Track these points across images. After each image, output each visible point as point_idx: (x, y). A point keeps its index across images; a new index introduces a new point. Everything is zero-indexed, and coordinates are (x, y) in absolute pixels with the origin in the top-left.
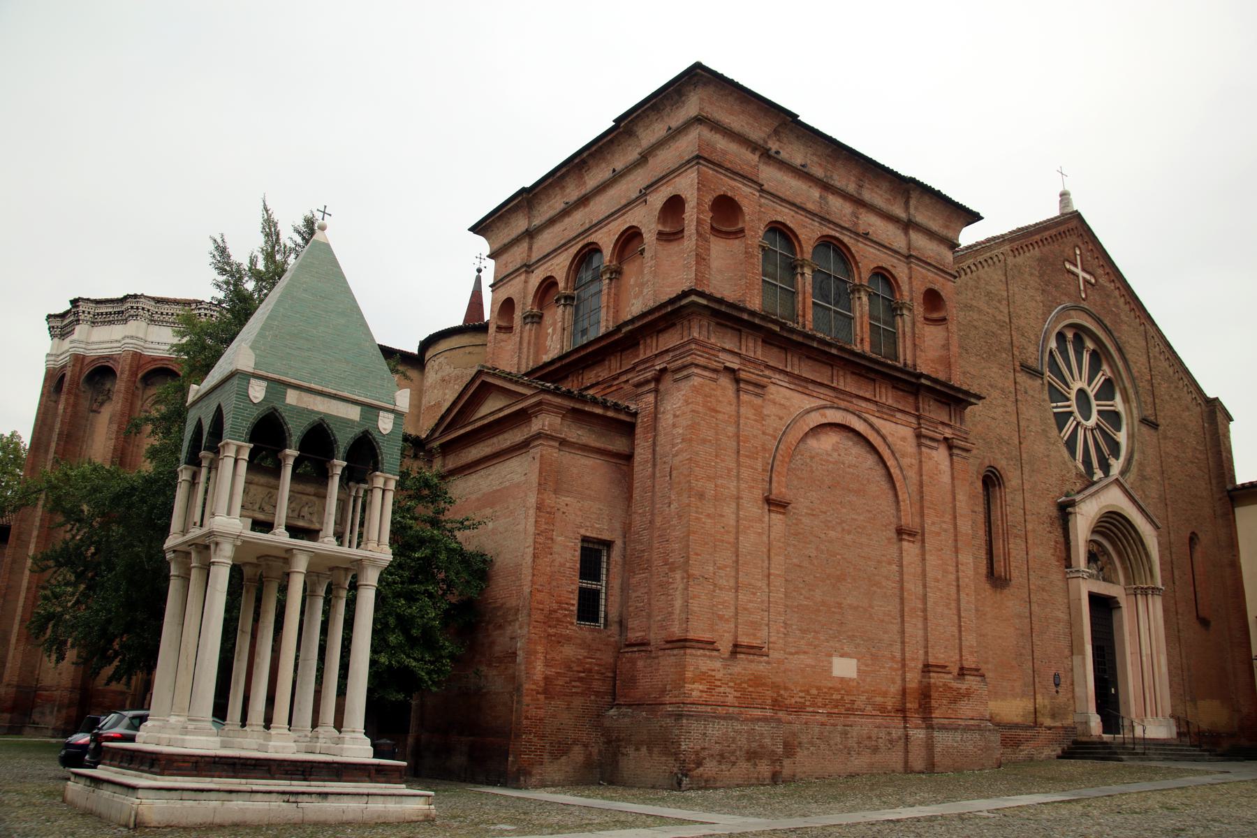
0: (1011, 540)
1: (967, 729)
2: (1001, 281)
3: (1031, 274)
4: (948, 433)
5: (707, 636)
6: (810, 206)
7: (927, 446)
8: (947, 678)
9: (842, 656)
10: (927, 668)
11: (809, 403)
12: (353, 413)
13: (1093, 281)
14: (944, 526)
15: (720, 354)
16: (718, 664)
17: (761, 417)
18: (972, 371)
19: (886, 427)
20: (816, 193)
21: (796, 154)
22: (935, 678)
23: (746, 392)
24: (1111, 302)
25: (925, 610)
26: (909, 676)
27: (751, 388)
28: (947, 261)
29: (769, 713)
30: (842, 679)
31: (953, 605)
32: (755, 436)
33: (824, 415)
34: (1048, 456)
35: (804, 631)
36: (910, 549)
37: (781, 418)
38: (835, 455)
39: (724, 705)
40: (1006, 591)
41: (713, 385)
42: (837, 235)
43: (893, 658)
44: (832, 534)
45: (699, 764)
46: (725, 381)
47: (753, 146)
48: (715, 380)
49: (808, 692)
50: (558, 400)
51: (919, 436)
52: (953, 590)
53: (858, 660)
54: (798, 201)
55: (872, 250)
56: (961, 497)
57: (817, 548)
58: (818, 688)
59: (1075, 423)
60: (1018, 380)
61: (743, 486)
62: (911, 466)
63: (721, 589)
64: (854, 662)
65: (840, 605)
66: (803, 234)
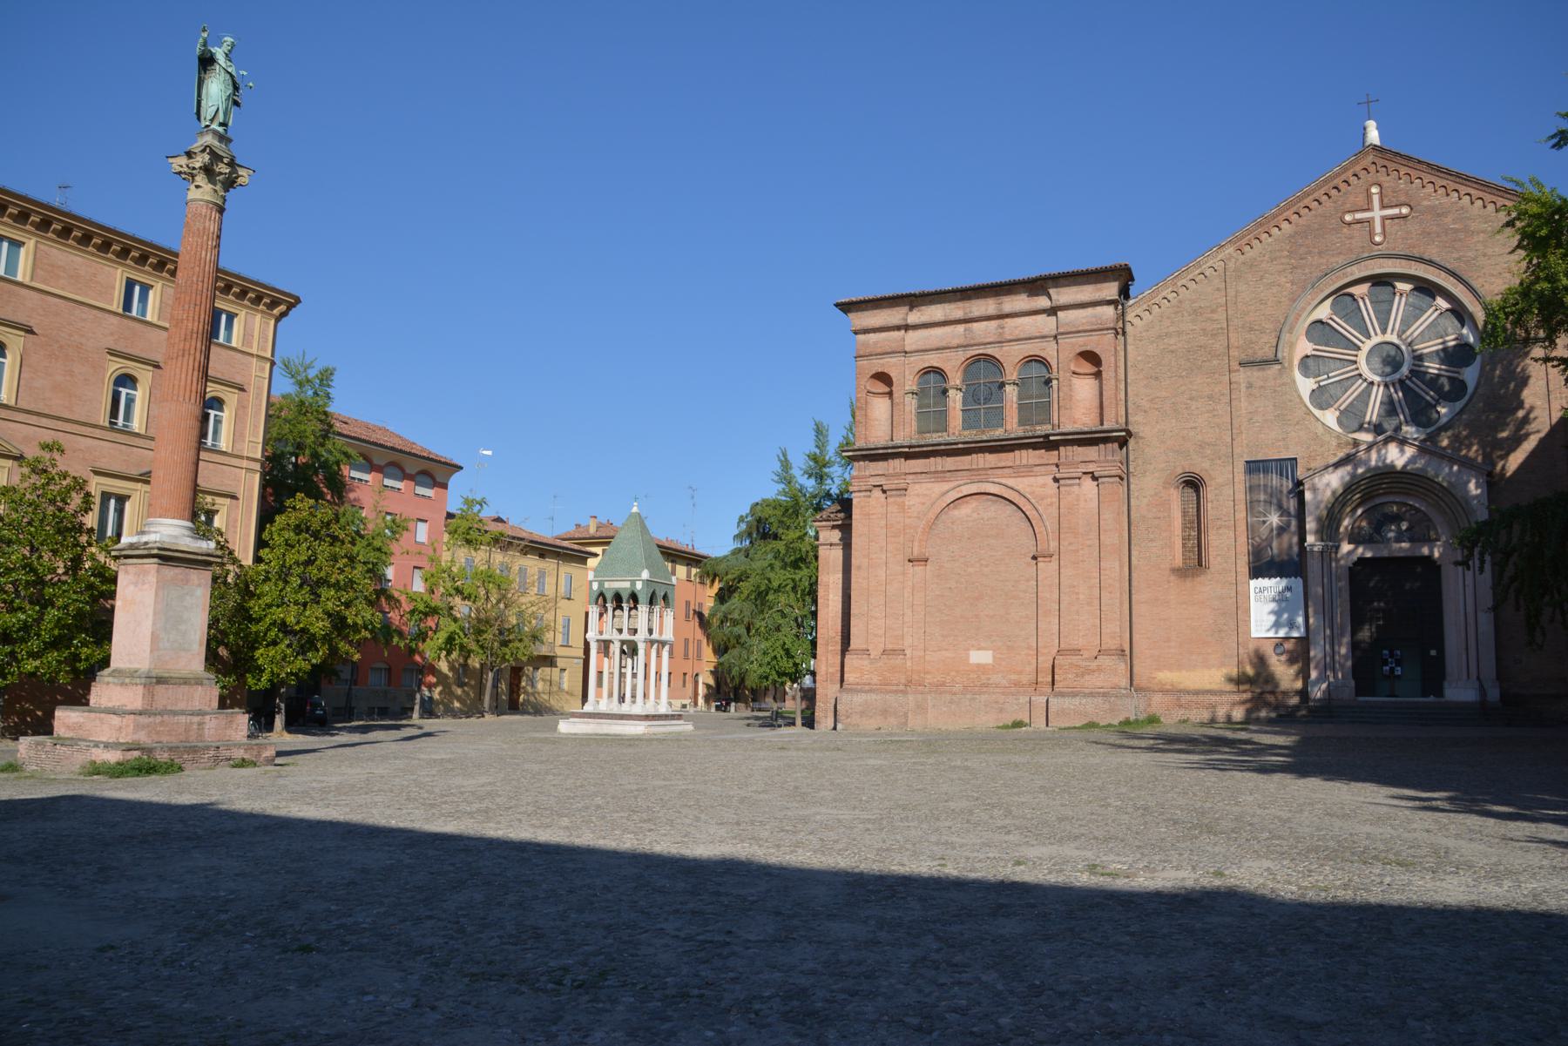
1: (1091, 695)
2: (1218, 289)
4: (1091, 467)
5: (864, 647)
6: (955, 342)
7: (1064, 485)
8: (1074, 659)
9: (979, 649)
11: (946, 486)
12: (627, 585)
13: (1405, 210)
14: (1088, 542)
15: (871, 479)
16: (866, 662)
17: (902, 508)
18: (1164, 394)
19: (1021, 483)
20: (960, 328)
21: (936, 312)
22: (1060, 660)
23: (891, 496)
24: (1449, 219)
27: (894, 492)
28: (1104, 317)
29: (902, 687)
30: (978, 666)
32: (899, 522)
33: (958, 492)
34: (1284, 439)
35: (943, 636)
36: (1047, 568)
37: (924, 504)
38: (975, 515)
39: (869, 684)
40: (1202, 578)
41: (868, 499)
42: (981, 352)
43: (1029, 648)
44: (971, 570)
45: (848, 717)
46: (877, 493)
47: (898, 328)
48: (870, 497)
49: (948, 674)
50: (824, 523)
51: (1056, 480)
53: (994, 651)
54: (944, 344)
55: (1017, 347)
56: (1107, 516)
57: (957, 582)
58: (957, 672)
59: (1365, 384)
60: (1233, 380)
61: (889, 555)
62: (1051, 504)
63: (876, 618)
64: (990, 653)
65: (977, 616)
66: (947, 367)
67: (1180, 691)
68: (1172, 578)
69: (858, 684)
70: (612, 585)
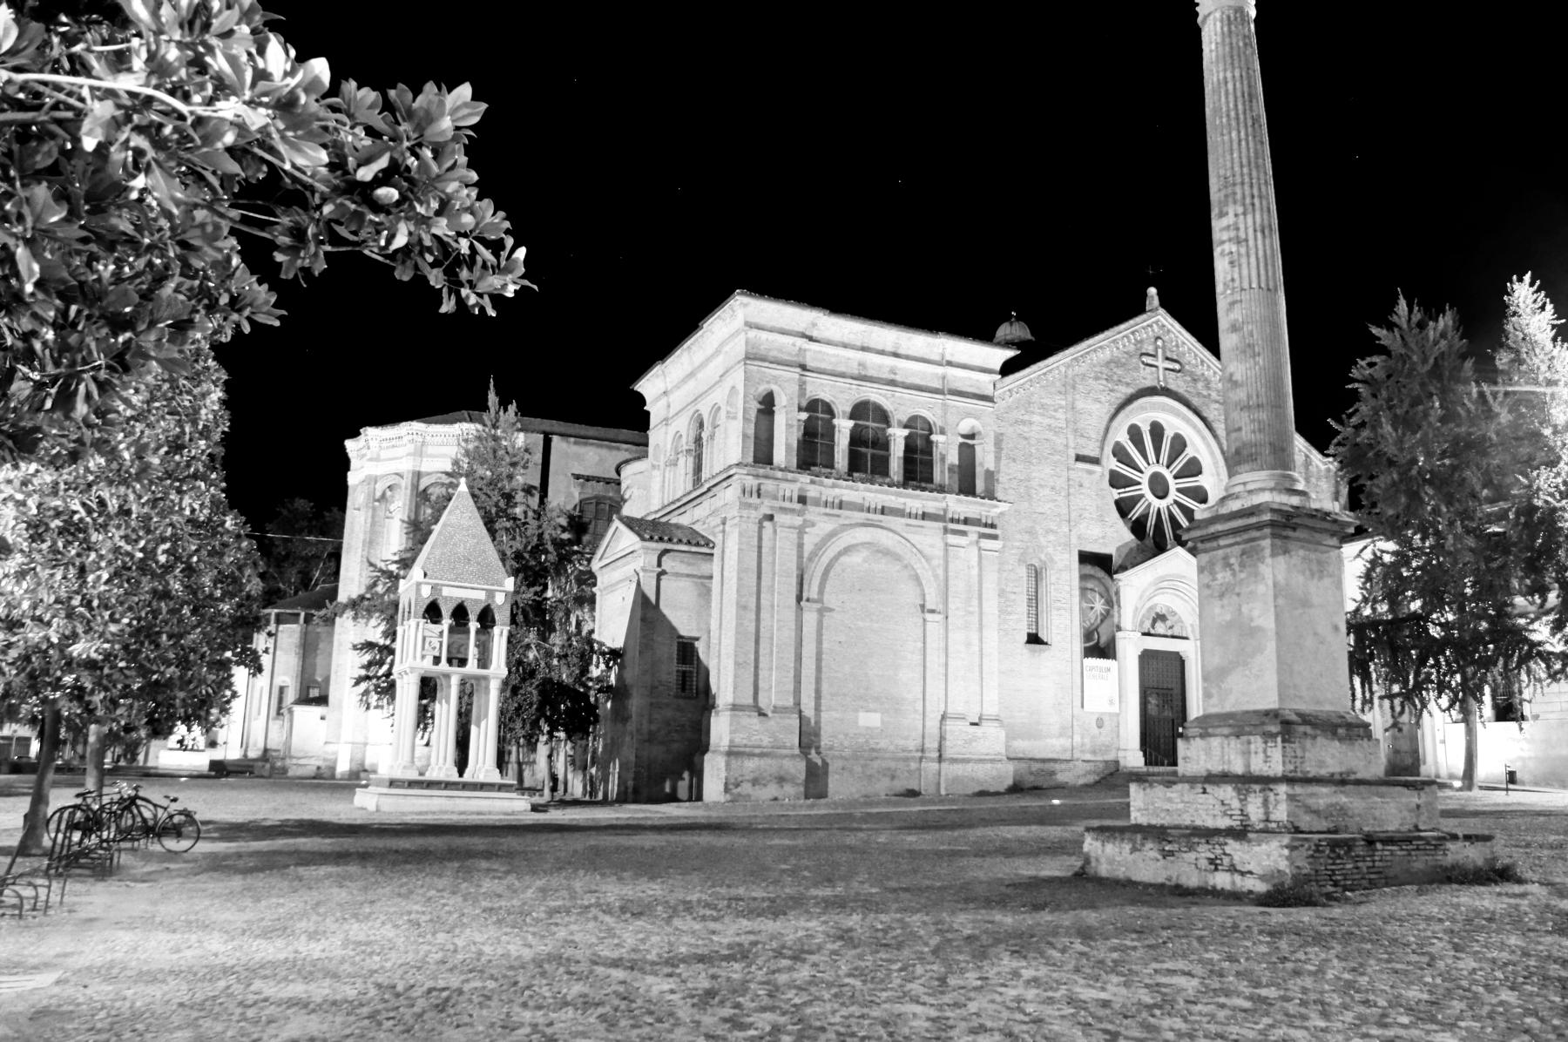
0: (1054, 612)
3: (1097, 378)
10: (944, 717)
12: (481, 595)
25: (946, 675)
26: (928, 724)
31: (977, 669)
39: (759, 747)
52: (977, 660)
67: (1031, 759)
68: (1025, 651)
69: (745, 746)
70: (452, 594)
